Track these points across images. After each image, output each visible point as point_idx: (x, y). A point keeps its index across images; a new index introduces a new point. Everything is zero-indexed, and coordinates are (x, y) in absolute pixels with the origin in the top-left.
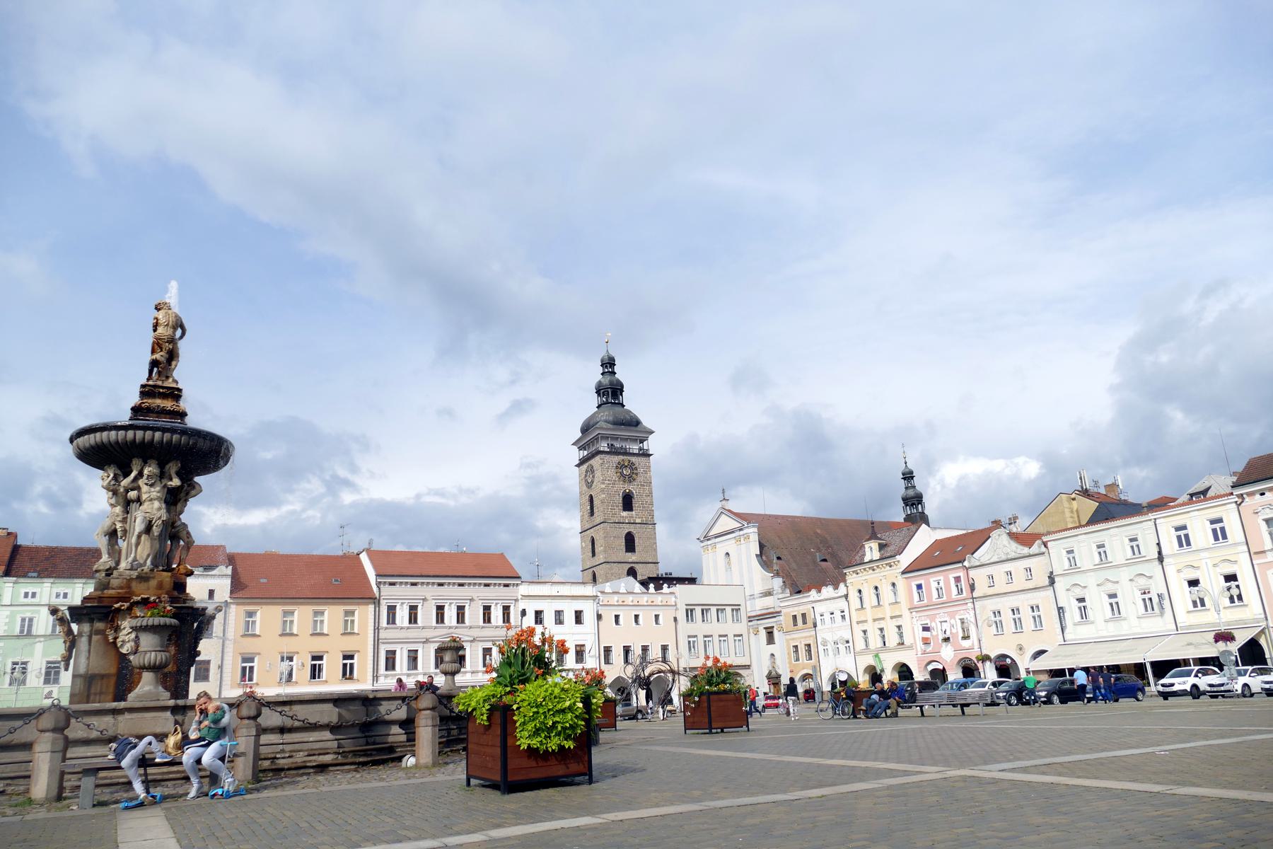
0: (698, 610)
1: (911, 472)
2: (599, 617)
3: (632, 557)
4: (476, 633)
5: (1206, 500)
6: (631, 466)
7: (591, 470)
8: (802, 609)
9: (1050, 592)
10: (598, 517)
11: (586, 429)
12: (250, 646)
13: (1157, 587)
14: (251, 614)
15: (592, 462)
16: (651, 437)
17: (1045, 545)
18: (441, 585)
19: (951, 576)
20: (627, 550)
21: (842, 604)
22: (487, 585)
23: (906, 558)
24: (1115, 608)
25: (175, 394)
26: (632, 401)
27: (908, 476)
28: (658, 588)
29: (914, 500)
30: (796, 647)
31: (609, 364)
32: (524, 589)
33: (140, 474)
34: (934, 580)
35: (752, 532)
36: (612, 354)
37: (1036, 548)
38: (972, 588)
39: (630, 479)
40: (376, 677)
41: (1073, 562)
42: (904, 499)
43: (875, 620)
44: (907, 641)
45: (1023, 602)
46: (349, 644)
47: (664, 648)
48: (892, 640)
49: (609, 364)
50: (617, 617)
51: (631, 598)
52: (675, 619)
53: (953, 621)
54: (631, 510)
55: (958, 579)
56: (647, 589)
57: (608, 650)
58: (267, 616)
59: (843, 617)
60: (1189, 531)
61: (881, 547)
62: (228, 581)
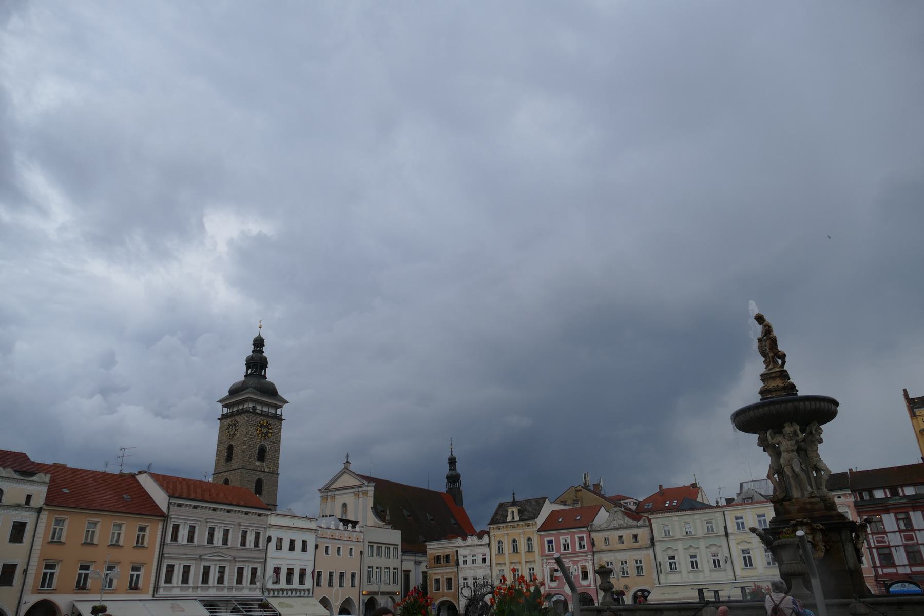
1: (455, 459)
2: (317, 547)
4: (235, 554)
5: (752, 503)
6: (267, 426)
7: (235, 425)
8: (447, 552)
9: (651, 552)
10: (236, 463)
12: (54, 552)
13: (723, 554)
14: (59, 522)
15: (238, 418)
16: (285, 405)
17: (650, 521)
18: (214, 510)
19: (576, 536)
21: (486, 550)
22: (247, 513)
24: (694, 565)
26: (272, 374)
27: (452, 462)
28: (353, 527)
29: (453, 479)
30: (437, 581)
31: (259, 343)
32: (273, 520)
34: (563, 538)
35: (371, 489)
37: (640, 523)
38: (593, 545)
40: (156, 589)
41: (667, 533)
42: (448, 478)
43: (512, 563)
45: (630, 556)
46: (138, 556)
47: (353, 575)
49: (259, 343)
50: (327, 547)
51: (337, 532)
52: (361, 553)
53: (576, 567)
55: (581, 539)
57: (319, 574)
58: (74, 526)
59: (484, 560)
60: (744, 520)
61: (520, 512)
62: (44, 489)
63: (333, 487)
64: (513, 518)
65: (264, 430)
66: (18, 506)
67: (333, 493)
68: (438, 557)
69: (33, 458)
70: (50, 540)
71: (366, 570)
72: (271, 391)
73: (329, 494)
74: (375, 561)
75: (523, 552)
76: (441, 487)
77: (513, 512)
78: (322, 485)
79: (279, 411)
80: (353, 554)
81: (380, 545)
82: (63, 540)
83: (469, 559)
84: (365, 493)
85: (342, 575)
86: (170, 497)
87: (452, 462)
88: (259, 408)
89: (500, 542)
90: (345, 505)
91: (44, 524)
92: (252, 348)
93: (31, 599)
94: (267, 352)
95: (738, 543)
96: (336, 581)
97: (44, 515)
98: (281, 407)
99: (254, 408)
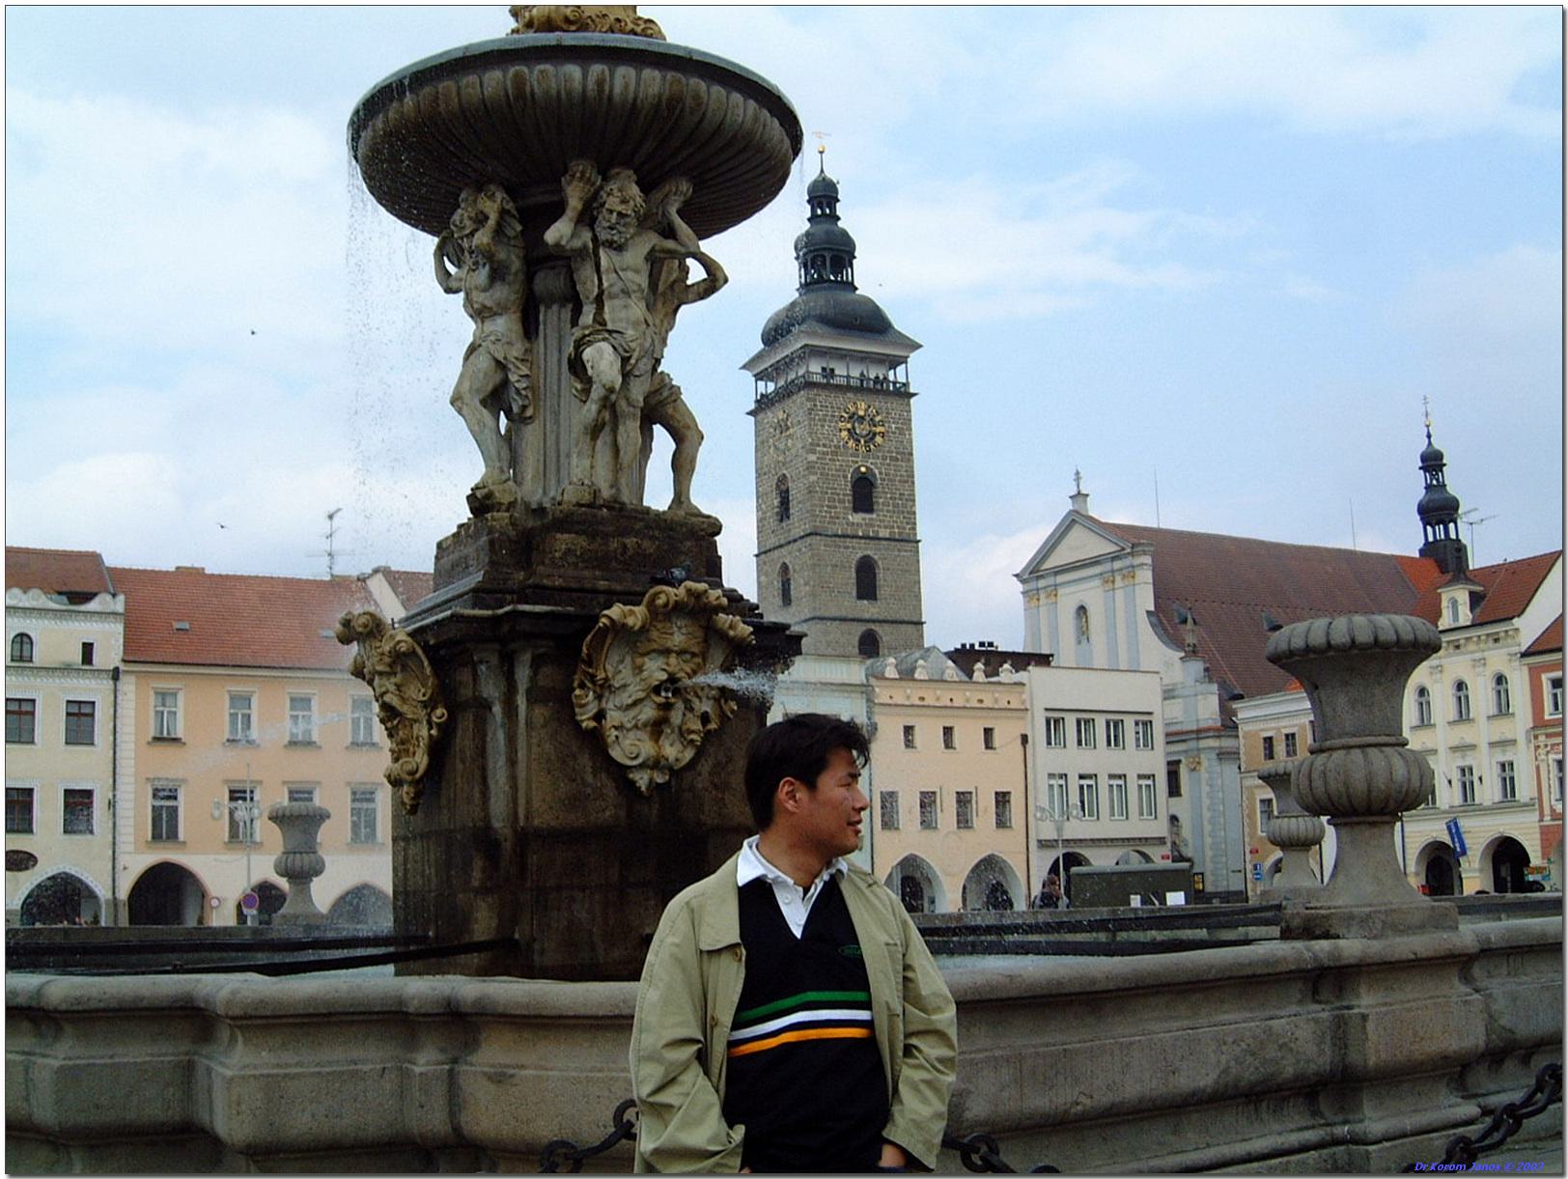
0: (1070, 721)
3: (867, 609)
8: (1288, 726)
10: (798, 525)
11: (774, 335)
12: (168, 765)
16: (914, 358)
20: (860, 597)
23: (1531, 625)
26: (873, 277)
27: (1432, 462)
29: (1438, 509)
36: (830, 174)
44: (1524, 790)
47: (1002, 799)
48: (1488, 791)
52: (1024, 739)
54: (870, 510)
56: (970, 674)
58: (200, 706)
61: (1475, 599)
62: (120, 628)
63: (1047, 565)
64: (1456, 617)
65: (862, 429)
66: (66, 669)
67: (1050, 581)
68: (1269, 741)
69: (111, 560)
70: (152, 733)
71: (1041, 784)
72: (871, 322)
73: (1042, 583)
75: (1482, 720)
76: (1406, 539)
77: (1454, 603)
78: (1022, 562)
80: (997, 741)
82: (180, 734)
84: (1130, 573)
85: (963, 799)
87: (1432, 462)
88: (840, 370)
90: (1082, 610)
91: (132, 705)
93: (137, 862)
96: (947, 812)
97: (128, 685)
98: (903, 360)
99: (828, 373)
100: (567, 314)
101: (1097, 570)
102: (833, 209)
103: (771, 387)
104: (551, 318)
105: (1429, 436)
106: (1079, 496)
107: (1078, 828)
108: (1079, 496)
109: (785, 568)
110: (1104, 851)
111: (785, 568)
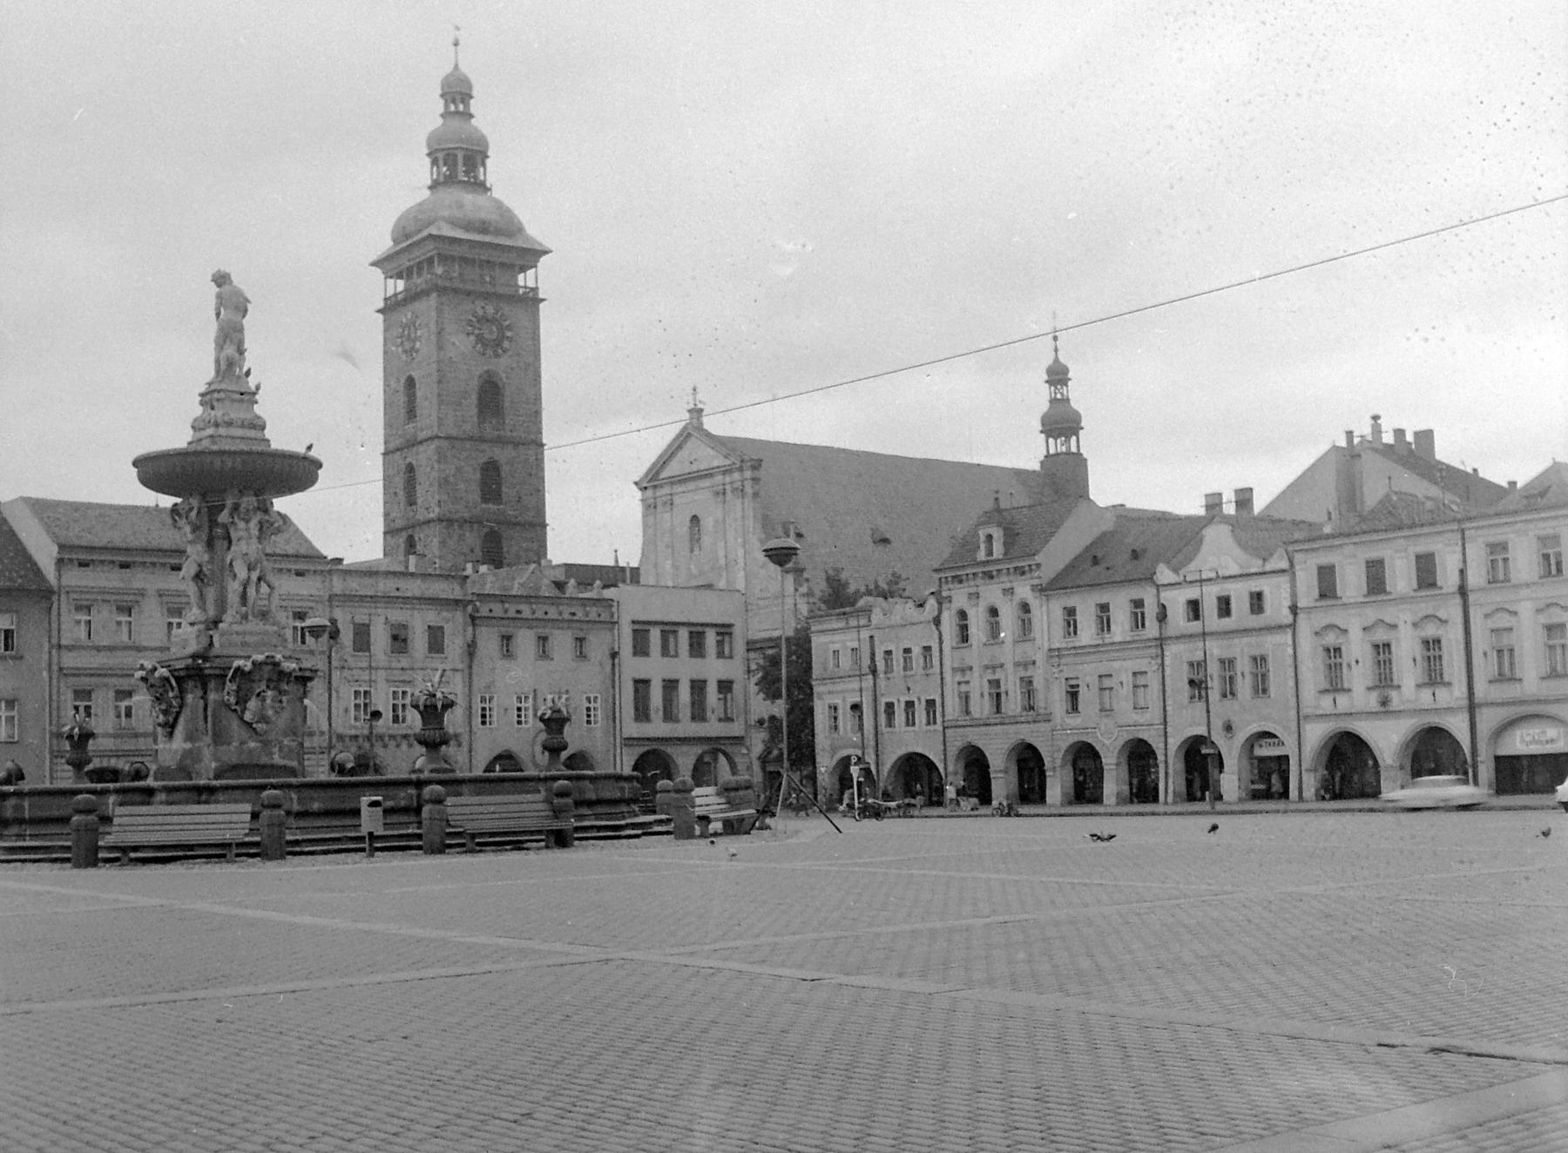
0: (655, 635)
1: (1065, 371)
25: (248, 397)
27: (1058, 376)
31: (457, 94)
33: (236, 508)
36: (464, 68)
38: (1162, 616)
39: (494, 346)
49: (457, 94)
59: (928, 663)
64: (990, 553)
74: (655, 668)
76: (1026, 451)
77: (990, 537)
78: (640, 470)
79: (525, 280)
81: (669, 629)
83: (898, 658)
86: (62, 547)
87: (1058, 376)
89: (963, 615)
90: (695, 519)
92: (440, 106)
94: (485, 117)
95: (1487, 616)
100: (226, 543)
101: (706, 483)
102: (467, 105)
103: (401, 285)
104: (220, 545)
105: (1056, 350)
106: (697, 412)
107: (657, 727)
108: (697, 412)
109: (410, 469)
110: (685, 748)
111: (410, 469)
